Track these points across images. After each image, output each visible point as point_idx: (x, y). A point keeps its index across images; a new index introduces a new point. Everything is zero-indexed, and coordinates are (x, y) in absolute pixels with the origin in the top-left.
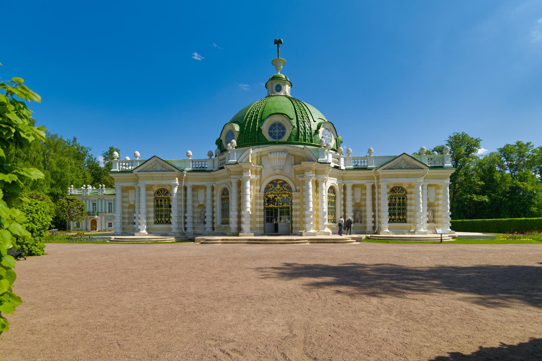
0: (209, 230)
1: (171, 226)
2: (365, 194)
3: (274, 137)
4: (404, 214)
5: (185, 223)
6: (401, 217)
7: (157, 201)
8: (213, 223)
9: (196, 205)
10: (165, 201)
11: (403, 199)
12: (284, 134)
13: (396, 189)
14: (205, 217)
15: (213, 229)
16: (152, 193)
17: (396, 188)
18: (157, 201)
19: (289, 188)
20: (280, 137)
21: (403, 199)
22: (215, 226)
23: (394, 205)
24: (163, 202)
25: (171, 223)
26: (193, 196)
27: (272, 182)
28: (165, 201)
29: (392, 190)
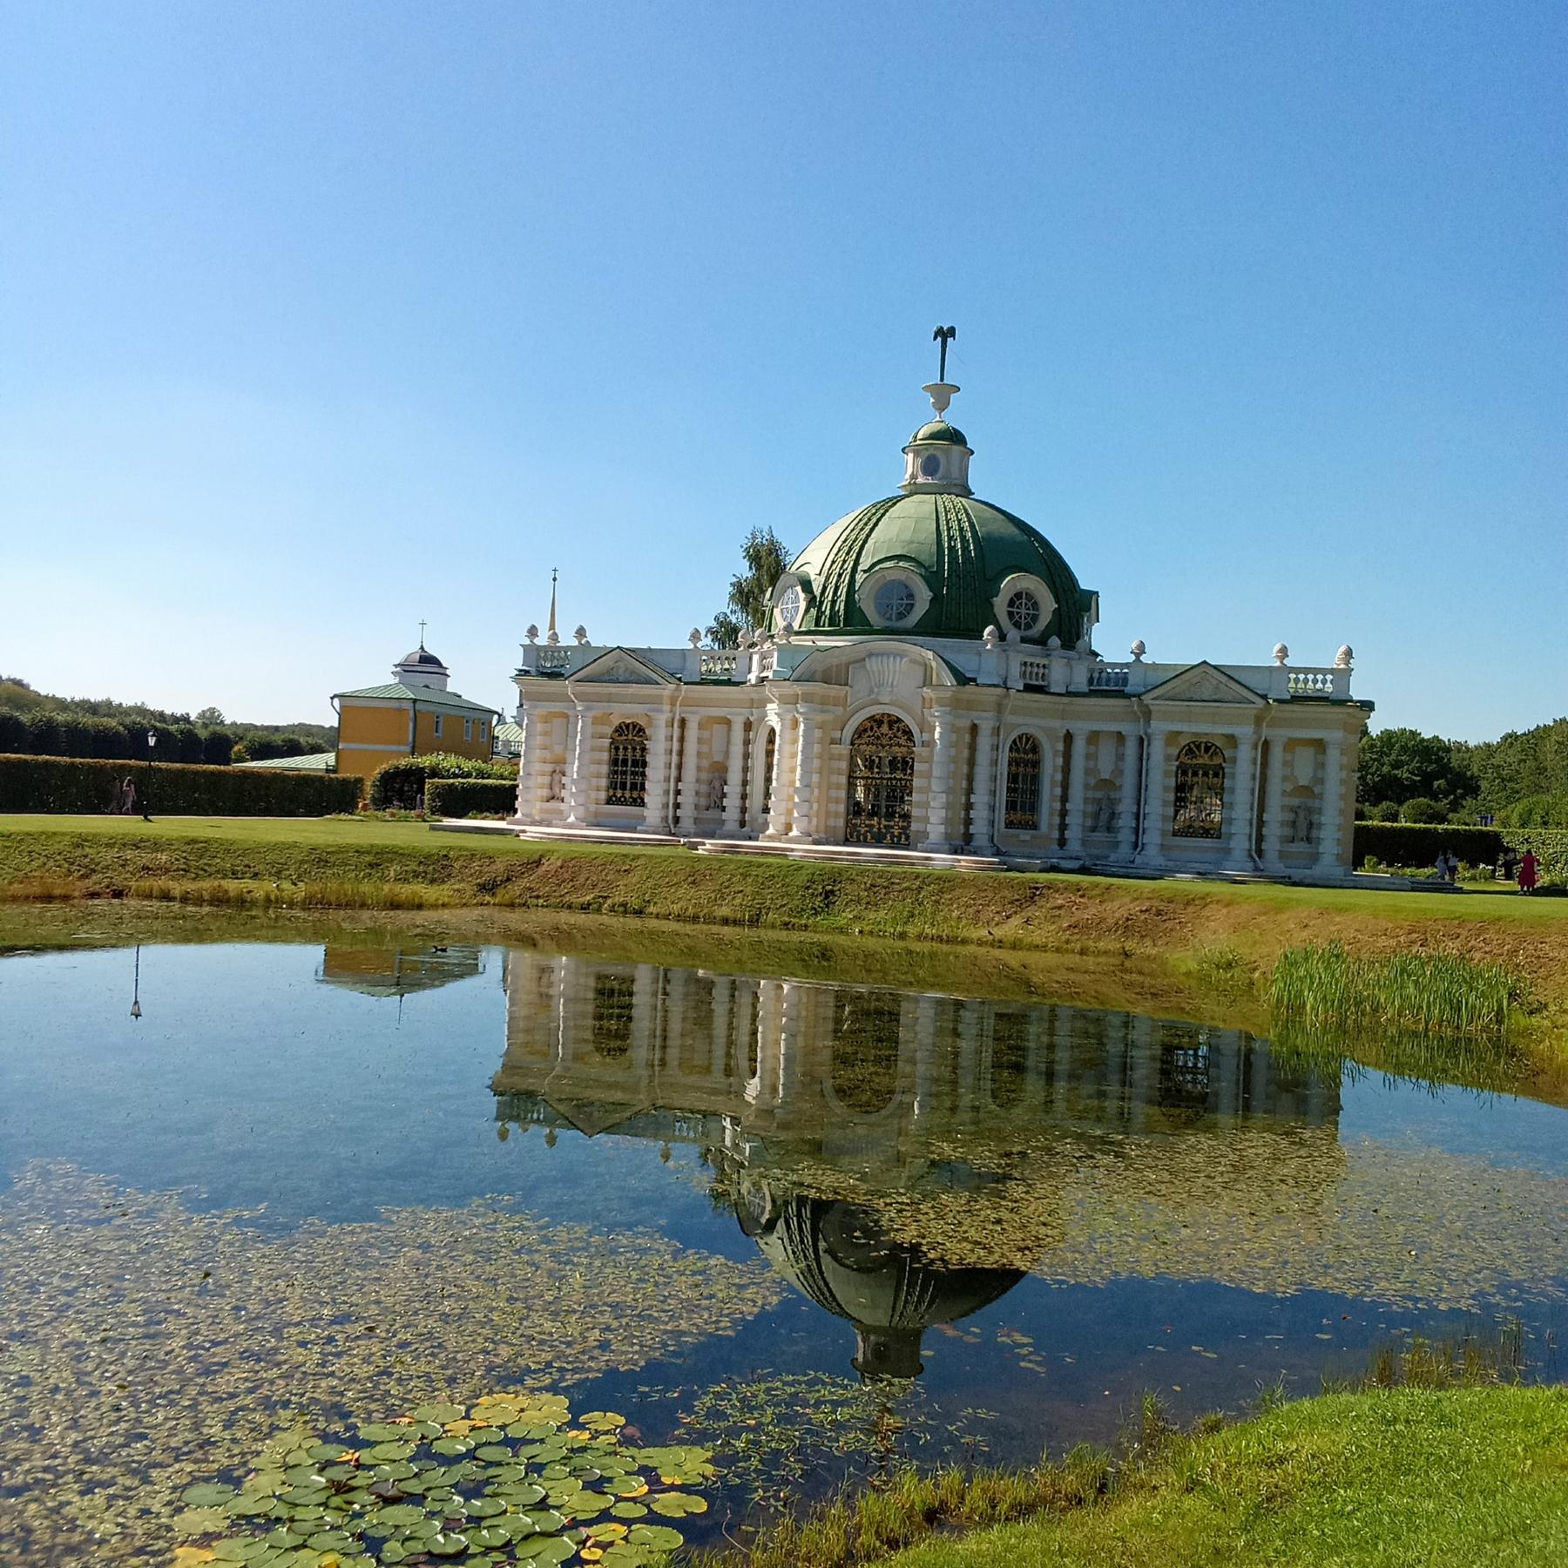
0: (731, 826)
1: (646, 812)
5: (677, 806)
7: (617, 749)
8: (744, 810)
13: (1198, 747)
14: (724, 795)
15: (743, 824)
16: (609, 730)
18: (617, 749)
19: (908, 733)
20: (901, 616)
25: (643, 804)
27: (872, 718)
28: (634, 749)
29: (1191, 750)
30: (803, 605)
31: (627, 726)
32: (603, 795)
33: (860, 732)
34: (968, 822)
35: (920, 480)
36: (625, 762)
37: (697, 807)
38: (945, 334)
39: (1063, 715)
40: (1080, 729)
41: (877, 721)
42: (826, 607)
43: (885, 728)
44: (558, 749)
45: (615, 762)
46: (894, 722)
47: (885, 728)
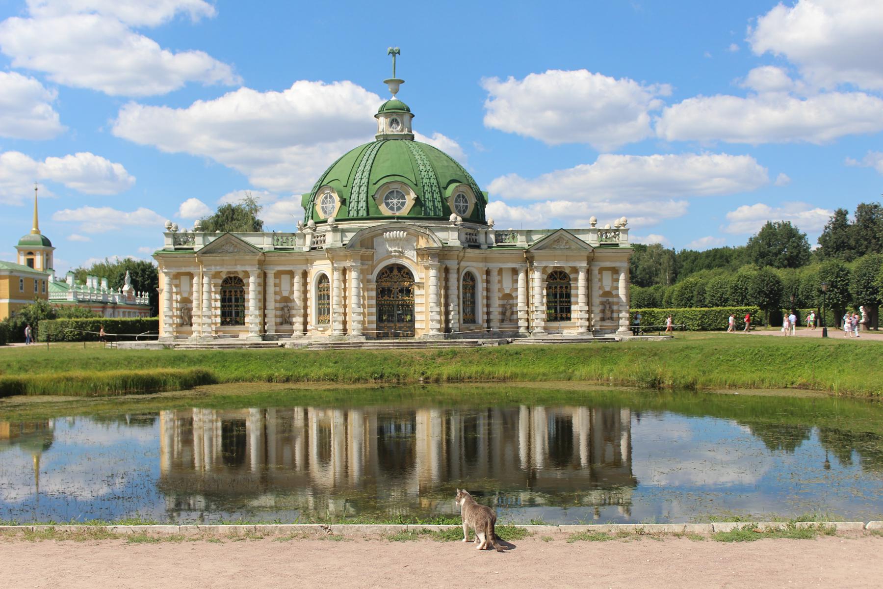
2: (517, 281)
3: (392, 209)
4: (569, 310)
6: (564, 315)
7: (225, 292)
9: (278, 298)
10: (236, 292)
11: (566, 287)
12: (403, 204)
16: (220, 281)
17: (556, 272)
18: (225, 292)
19: (410, 275)
20: (399, 209)
21: (566, 287)
22: (309, 327)
23: (555, 296)
24: (233, 293)
26: (275, 285)
30: (338, 204)
31: (231, 278)
32: (219, 320)
33: (381, 274)
34: (447, 321)
35: (389, 131)
36: (230, 300)
37: (276, 324)
38: (393, 53)
39: (486, 260)
40: (494, 266)
41: (390, 268)
42: (353, 204)
43: (395, 272)
44: (186, 295)
45: (223, 300)
46: (401, 268)
47: (395, 272)
